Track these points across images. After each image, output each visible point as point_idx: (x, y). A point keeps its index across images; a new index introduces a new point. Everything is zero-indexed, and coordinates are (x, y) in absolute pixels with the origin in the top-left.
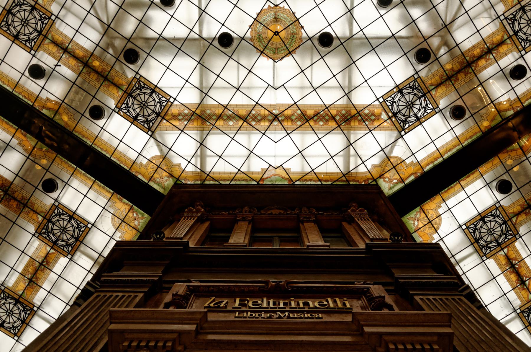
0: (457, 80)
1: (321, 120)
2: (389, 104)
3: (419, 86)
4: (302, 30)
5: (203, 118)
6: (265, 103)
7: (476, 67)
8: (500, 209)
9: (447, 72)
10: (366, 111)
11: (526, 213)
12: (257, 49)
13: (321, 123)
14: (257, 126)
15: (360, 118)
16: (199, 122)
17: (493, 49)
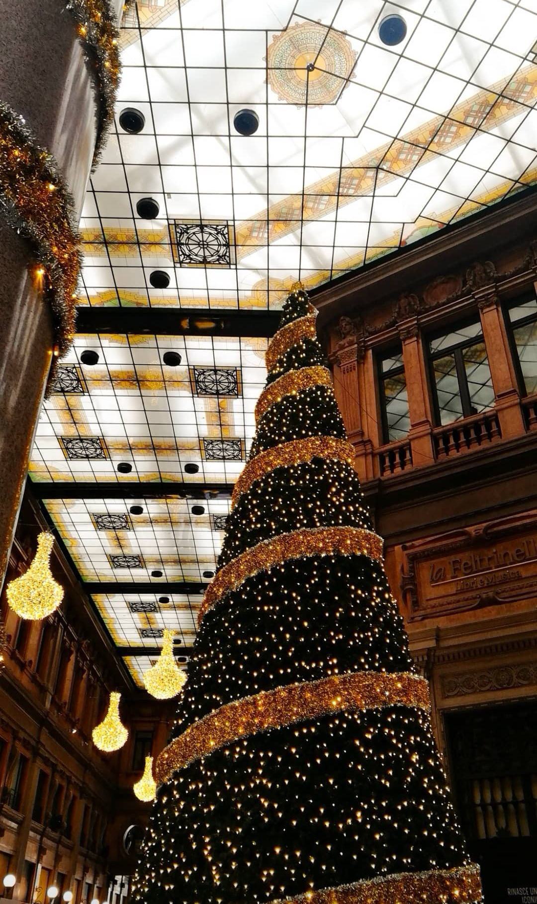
1: (446, 137)
4: (347, 38)
5: (282, 219)
6: (352, 160)
10: (513, 86)
12: (296, 104)
13: (448, 140)
14: (359, 193)
15: (506, 101)
16: (281, 225)
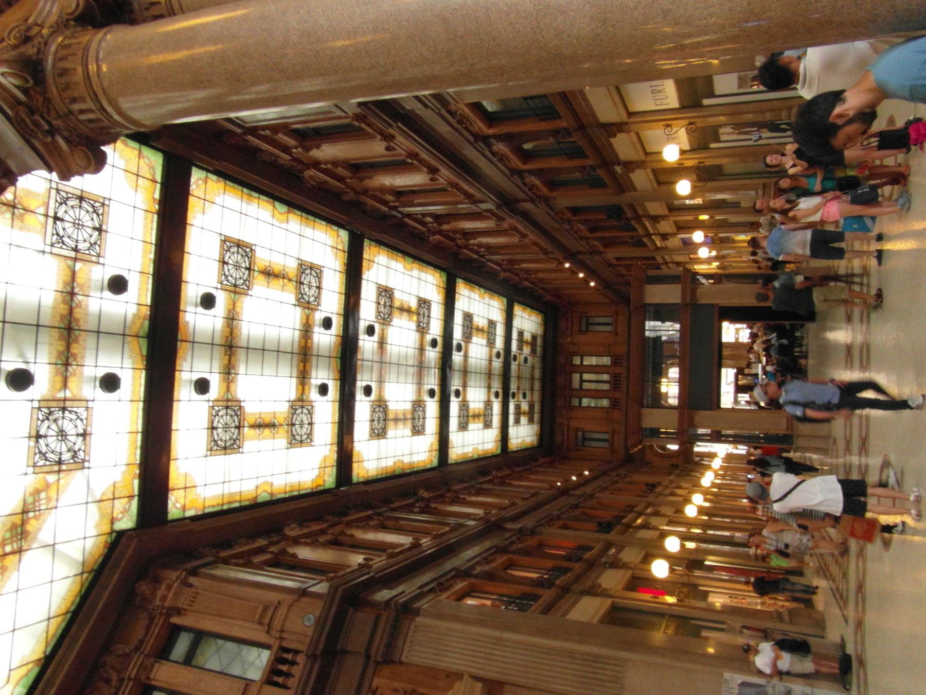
0: (75, 356)
2: (42, 463)
3: (49, 408)
7: (77, 324)
8: (216, 403)
9: (60, 362)
10: (30, 500)
11: (232, 381)
15: (31, 514)
17: (73, 288)
